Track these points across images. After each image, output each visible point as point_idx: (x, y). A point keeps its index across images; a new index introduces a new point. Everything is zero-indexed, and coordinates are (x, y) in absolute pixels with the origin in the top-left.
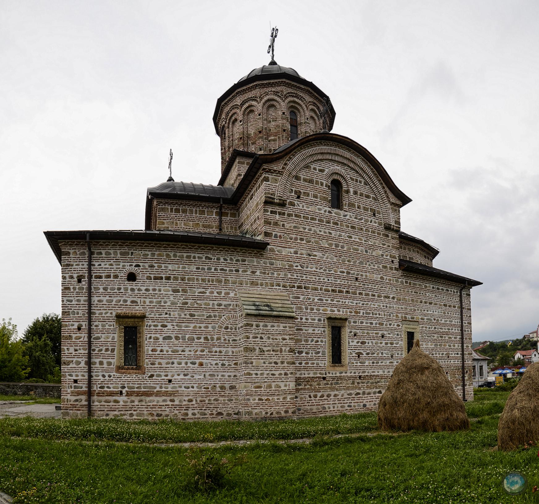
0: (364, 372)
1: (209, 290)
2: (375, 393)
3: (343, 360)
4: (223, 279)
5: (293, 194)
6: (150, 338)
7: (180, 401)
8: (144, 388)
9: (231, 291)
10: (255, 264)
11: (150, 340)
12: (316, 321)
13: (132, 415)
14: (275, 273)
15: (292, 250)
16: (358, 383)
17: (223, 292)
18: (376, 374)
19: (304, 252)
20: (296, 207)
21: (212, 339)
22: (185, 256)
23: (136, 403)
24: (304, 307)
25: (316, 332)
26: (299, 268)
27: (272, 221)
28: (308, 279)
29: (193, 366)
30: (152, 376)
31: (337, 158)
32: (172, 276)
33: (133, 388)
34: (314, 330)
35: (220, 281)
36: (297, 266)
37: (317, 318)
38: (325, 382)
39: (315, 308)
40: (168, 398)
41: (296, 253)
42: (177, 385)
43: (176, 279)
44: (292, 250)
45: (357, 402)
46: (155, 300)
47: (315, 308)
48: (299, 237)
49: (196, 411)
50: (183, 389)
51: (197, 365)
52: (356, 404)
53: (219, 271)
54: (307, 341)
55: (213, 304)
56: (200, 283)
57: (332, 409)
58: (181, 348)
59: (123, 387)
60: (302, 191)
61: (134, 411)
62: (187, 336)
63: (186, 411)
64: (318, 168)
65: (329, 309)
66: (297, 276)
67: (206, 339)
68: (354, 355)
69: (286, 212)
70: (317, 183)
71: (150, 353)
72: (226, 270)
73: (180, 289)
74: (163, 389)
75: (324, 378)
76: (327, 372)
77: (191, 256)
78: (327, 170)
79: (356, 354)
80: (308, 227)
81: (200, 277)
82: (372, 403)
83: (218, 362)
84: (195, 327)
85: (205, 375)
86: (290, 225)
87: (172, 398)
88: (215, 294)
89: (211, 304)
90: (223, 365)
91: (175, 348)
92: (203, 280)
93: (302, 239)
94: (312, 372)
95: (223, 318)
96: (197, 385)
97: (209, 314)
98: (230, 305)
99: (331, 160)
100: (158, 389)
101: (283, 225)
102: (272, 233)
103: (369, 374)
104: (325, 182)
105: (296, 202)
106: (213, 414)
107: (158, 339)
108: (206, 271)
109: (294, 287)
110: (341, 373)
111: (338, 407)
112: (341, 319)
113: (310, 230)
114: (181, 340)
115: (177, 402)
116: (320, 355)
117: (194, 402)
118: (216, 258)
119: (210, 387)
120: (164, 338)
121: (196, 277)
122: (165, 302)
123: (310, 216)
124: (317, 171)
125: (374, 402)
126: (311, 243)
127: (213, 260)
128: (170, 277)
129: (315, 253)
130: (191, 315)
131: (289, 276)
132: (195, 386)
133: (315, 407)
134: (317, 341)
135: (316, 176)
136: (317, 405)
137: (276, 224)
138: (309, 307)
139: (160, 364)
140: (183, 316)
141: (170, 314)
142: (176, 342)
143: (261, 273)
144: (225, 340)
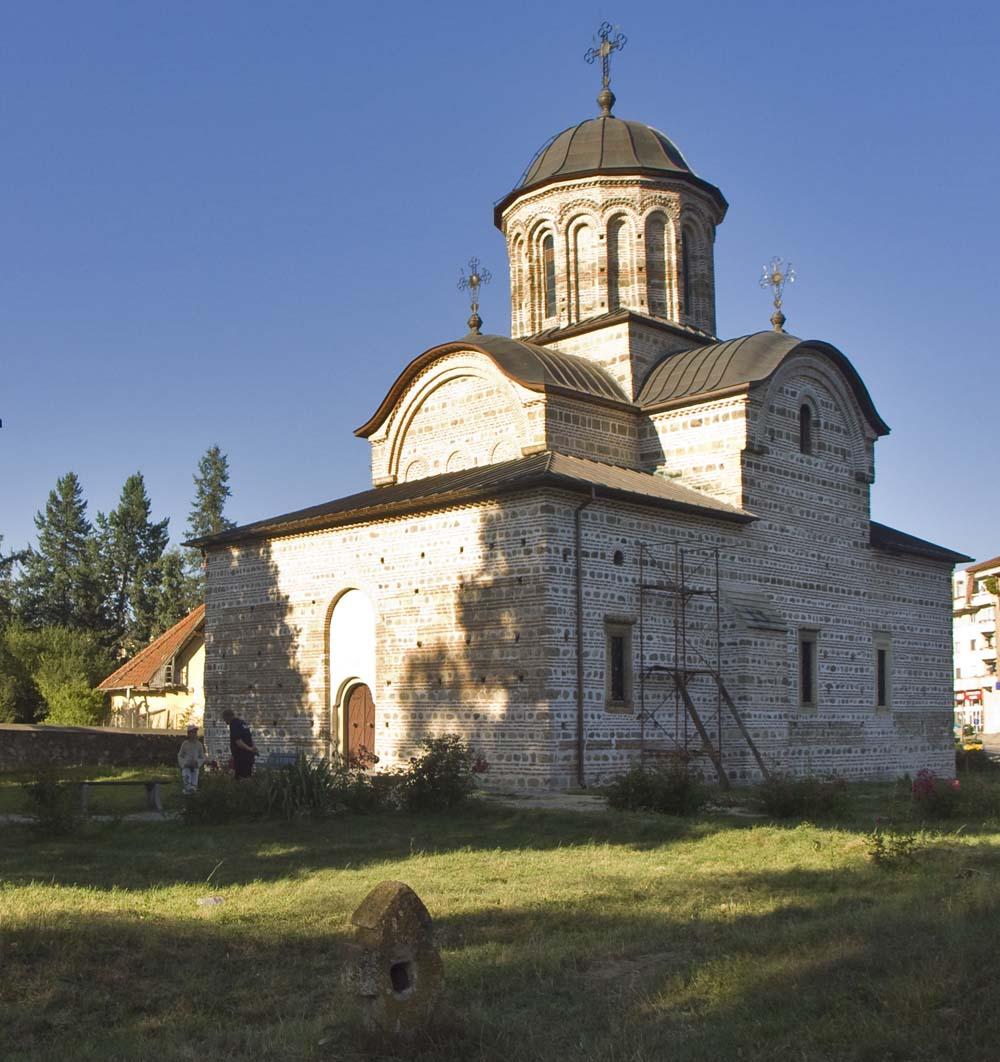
0: (834, 717)
15: (767, 523)
26: (773, 551)
41: (770, 527)
59: (612, 735)
90: (704, 700)
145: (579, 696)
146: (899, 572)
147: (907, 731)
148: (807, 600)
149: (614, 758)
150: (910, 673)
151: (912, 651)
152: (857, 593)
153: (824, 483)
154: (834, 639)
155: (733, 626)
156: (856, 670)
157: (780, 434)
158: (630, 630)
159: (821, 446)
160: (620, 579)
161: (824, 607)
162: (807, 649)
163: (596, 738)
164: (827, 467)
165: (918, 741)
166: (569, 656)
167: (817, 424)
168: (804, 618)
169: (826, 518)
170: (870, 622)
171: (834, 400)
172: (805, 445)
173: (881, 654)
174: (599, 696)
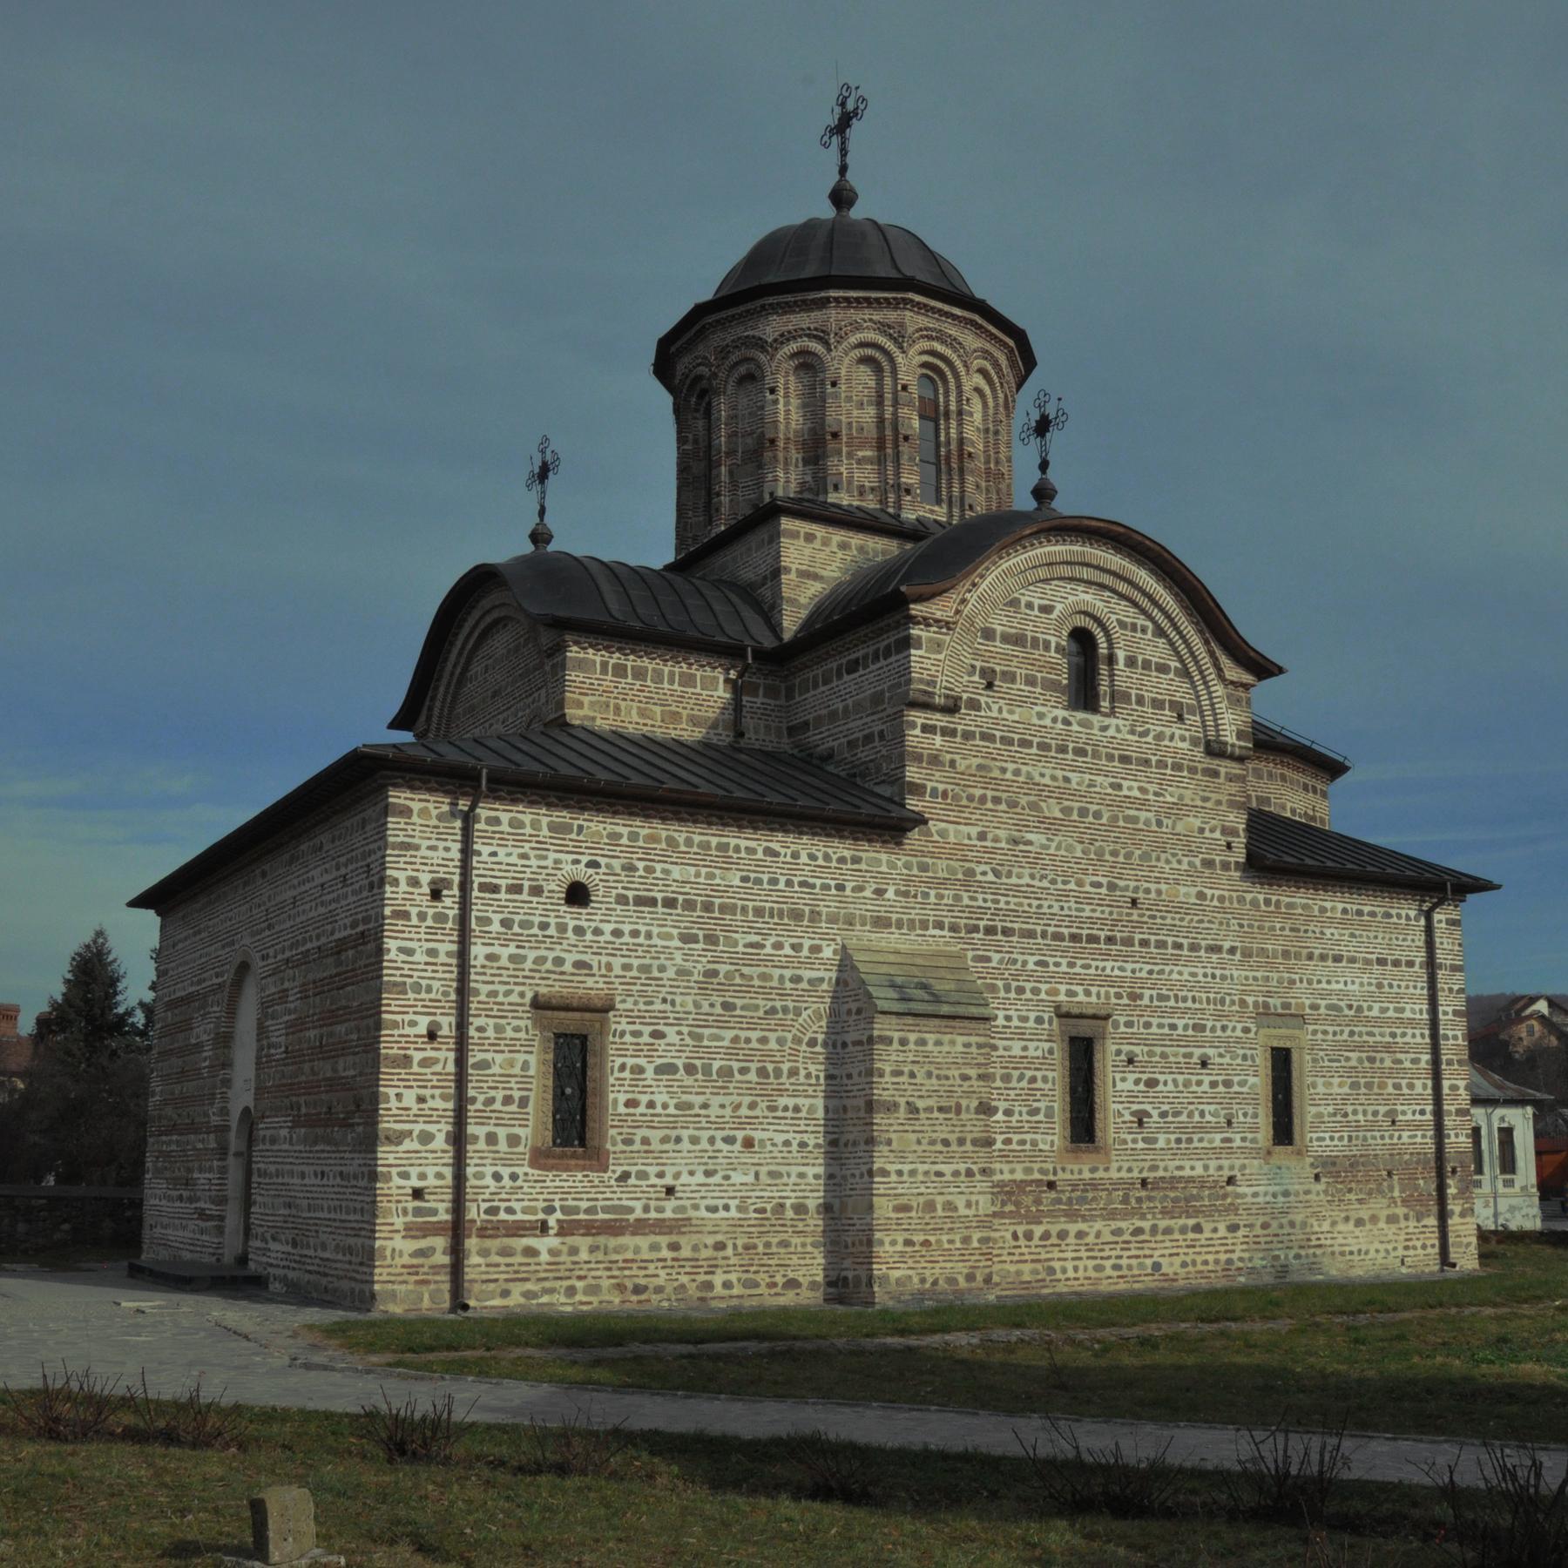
0: (1154, 1168)
1: (773, 940)
2: (1183, 1230)
3: (1098, 1134)
4: (807, 909)
5: (976, 678)
6: (623, 1068)
7: (695, 1248)
8: (605, 1210)
9: (824, 943)
10: (884, 869)
11: (622, 1075)
12: (1031, 1024)
13: (571, 1291)
14: (933, 893)
15: (974, 831)
16: (1139, 1200)
17: (807, 943)
18: (1187, 1173)
19: (1002, 834)
21: (778, 1073)
22: (713, 845)
23: (584, 1255)
24: (1000, 983)
25: (1031, 1053)
28: (1012, 907)
29: (729, 1147)
30: (625, 1176)
32: (681, 898)
33: (576, 1210)
34: (1025, 1048)
35: (797, 915)
36: (984, 873)
37: (1032, 1016)
38: (1053, 1195)
39: (1028, 986)
40: (664, 1240)
41: (982, 836)
42: (688, 1203)
43: (689, 905)
45: (1137, 1257)
46: (636, 963)
47: (1028, 986)
48: (990, 794)
49: (733, 1277)
50: (704, 1213)
51: (738, 1146)
52: (1134, 1262)
53: (797, 888)
54: (1006, 1078)
55: (782, 977)
56: (751, 918)
57: (1071, 1274)
58: (699, 1100)
59: (550, 1210)
60: (998, 668)
61: (580, 1278)
62: (716, 1065)
63: (708, 1277)
64: (1037, 602)
65: (1063, 988)
66: (985, 901)
67: (762, 1072)
68: (1128, 1117)
69: (960, 728)
71: (622, 1109)
72: (813, 886)
73: (701, 933)
74: (653, 1215)
75: (1051, 1185)
76: (1059, 1167)
78: (1059, 607)
79: (1133, 1114)
80: (1011, 767)
81: (750, 904)
82: (1177, 1261)
83: (789, 1136)
84: (735, 1039)
85: (757, 1175)
87: (674, 1238)
88: (788, 951)
89: (776, 977)
90: (803, 1145)
91: (685, 1098)
92: (759, 912)
93: (997, 800)
94: (1019, 1167)
95: (805, 1014)
96: (737, 1202)
97: (770, 1004)
98: (822, 980)
100: (638, 1213)
101: (952, 763)
102: (924, 787)
103: (1168, 1174)
104: (1053, 640)
105: (983, 700)
106: (775, 1285)
107: (641, 1070)
109: (976, 929)
110: (1094, 1170)
111: (1086, 1269)
112: (1095, 1017)
113: (1017, 772)
114: (700, 1076)
115: (686, 1252)
116: (1041, 1117)
117: (729, 1251)
118: (789, 852)
119: (769, 1207)
120: (659, 1070)
121: (740, 903)
122: (662, 969)
123: (1016, 737)
124: (1036, 612)
125: (1182, 1257)
126: (1018, 810)
127: (781, 859)
128: (675, 900)
129: (1029, 836)
130: (727, 1006)
131: (966, 901)
132: (733, 1203)
133: (1027, 1268)
134: (1033, 1080)
136: (1033, 1261)
137: (935, 760)
138: (1014, 984)
139: (645, 1141)
140: (706, 1008)
141: (673, 1003)
142: (689, 1081)
143: (897, 893)
144: (808, 1076)
145: (459, 1139)
146: (1323, 910)
147: (1350, 1191)
148: (1079, 963)
149: (551, 1252)
150: (1355, 1085)
151: (1359, 1047)
152: (1215, 949)
153: (1125, 759)
154: (1154, 1029)
155: (859, 1012)
156: (1213, 1084)
157: (1010, 677)
158: (604, 1023)
159: (1117, 697)
160: (579, 931)
161: (1129, 974)
162: (1082, 1056)
163: (503, 1216)
164: (1132, 732)
165: (1379, 1206)
166: (438, 1068)
167: (1111, 659)
168: (1071, 993)
169: (1135, 820)
170: (1250, 1000)
171: (1150, 617)
173: (1282, 1061)
174: (513, 1140)
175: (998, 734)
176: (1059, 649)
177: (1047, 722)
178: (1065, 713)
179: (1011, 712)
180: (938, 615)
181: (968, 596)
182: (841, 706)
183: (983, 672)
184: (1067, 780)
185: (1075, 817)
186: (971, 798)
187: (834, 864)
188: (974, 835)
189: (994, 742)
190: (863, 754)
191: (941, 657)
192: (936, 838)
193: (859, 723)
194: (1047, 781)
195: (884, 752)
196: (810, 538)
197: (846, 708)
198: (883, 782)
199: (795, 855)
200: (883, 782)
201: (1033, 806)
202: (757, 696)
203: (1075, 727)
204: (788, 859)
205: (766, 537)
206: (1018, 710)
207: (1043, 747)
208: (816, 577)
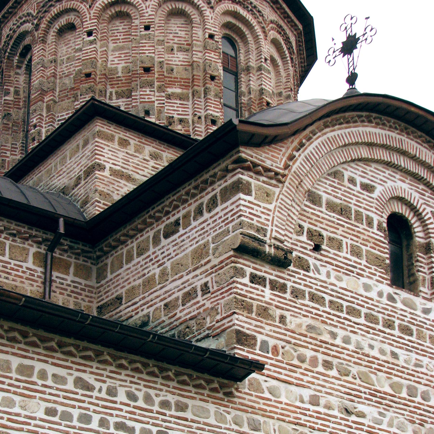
5: (304, 238)
15: (306, 393)
19: (334, 401)
20: (311, 274)
27: (255, 303)
31: (402, 162)
41: (314, 401)
44: (306, 393)
48: (321, 357)
60: (324, 233)
64: (359, 180)
69: (289, 284)
70: (359, 217)
77: (32, 368)
80: (341, 333)
86: (298, 321)
93: (328, 365)
99: (388, 164)
101: (282, 319)
102: (254, 338)
104: (376, 219)
105: (311, 261)
108: (75, 423)
113: (347, 340)
118: (105, 387)
123: (345, 304)
124: (358, 188)
126: (349, 379)
127: (95, 393)
135: (357, 201)
137: (264, 312)
172: (401, 274)
175: (327, 298)
176: (380, 228)
177: (373, 294)
178: (391, 290)
179: (339, 279)
180: (268, 164)
181: (297, 154)
182: (157, 271)
183: (311, 234)
184: (394, 355)
185: (404, 394)
186: (302, 359)
187: (156, 408)
188: (306, 398)
189: (324, 305)
190: (183, 313)
191: (271, 207)
192: (267, 395)
193: (179, 282)
194: (375, 353)
195: (208, 305)
196: (124, 143)
197: (164, 274)
198: (207, 336)
199: (112, 392)
200: (207, 336)
201: (363, 377)
202: (68, 274)
203: (399, 305)
204: (103, 395)
205: (81, 142)
206: (345, 277)
207: (370, 318)
208: (129, 178)
